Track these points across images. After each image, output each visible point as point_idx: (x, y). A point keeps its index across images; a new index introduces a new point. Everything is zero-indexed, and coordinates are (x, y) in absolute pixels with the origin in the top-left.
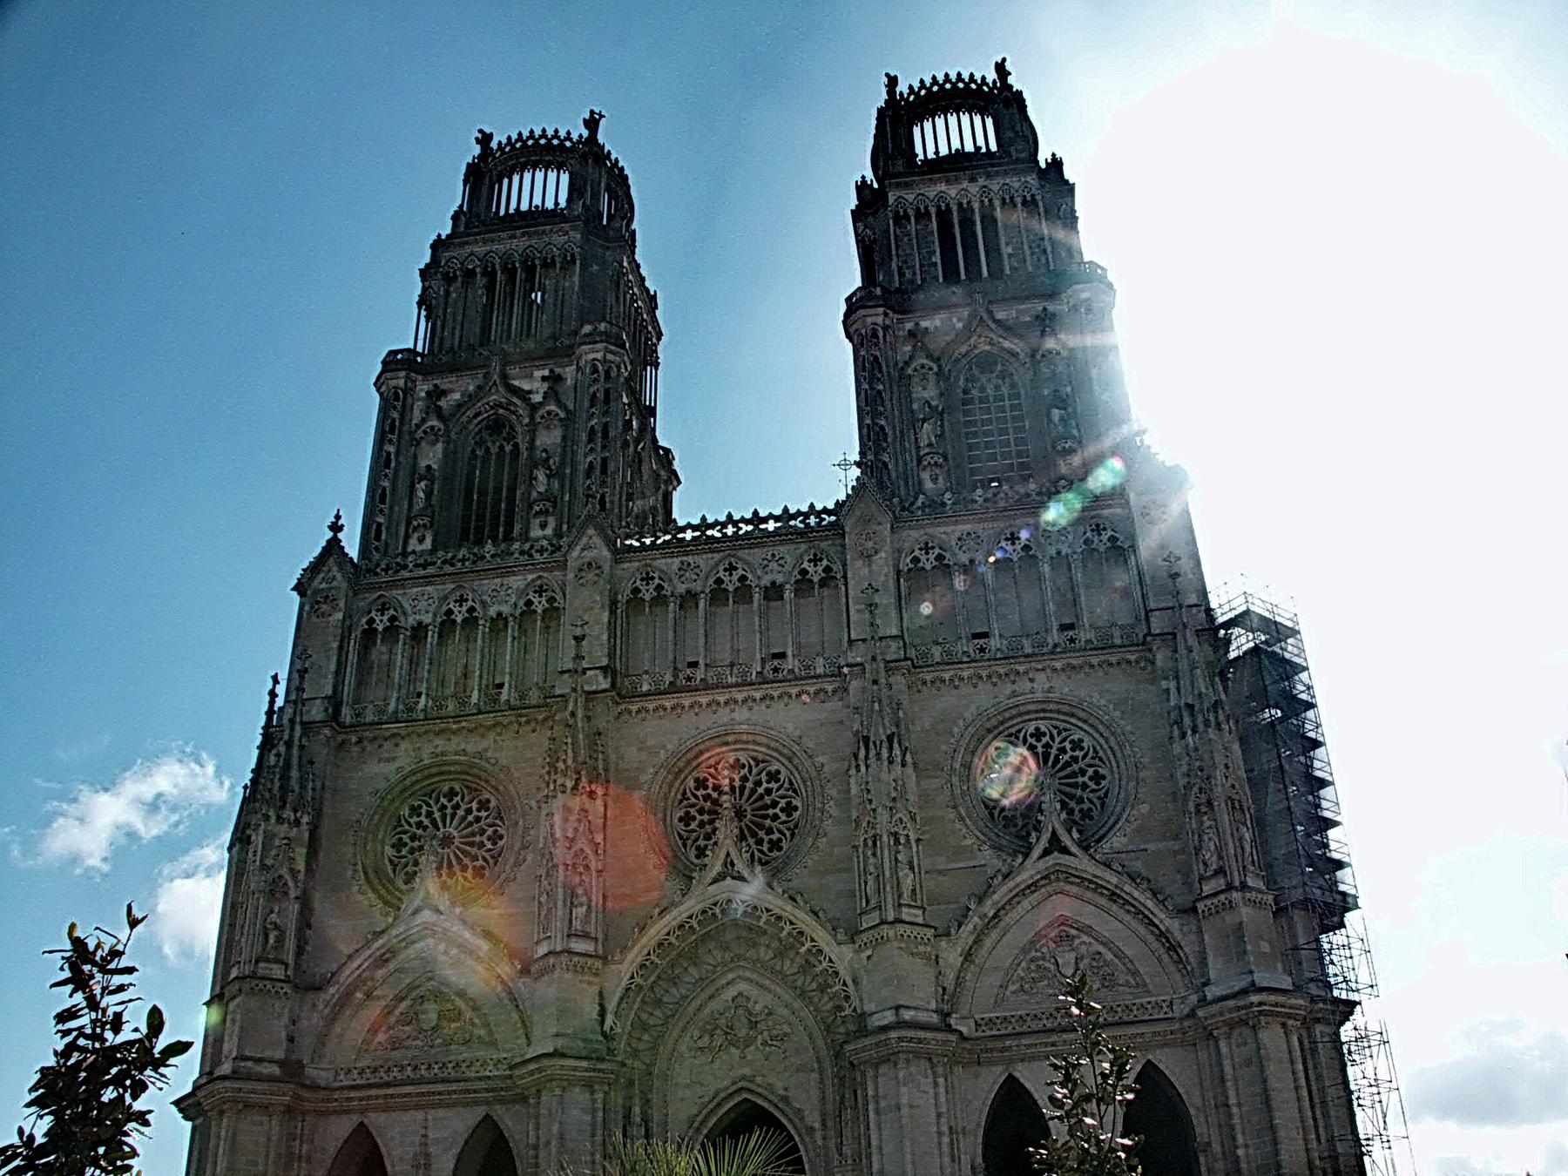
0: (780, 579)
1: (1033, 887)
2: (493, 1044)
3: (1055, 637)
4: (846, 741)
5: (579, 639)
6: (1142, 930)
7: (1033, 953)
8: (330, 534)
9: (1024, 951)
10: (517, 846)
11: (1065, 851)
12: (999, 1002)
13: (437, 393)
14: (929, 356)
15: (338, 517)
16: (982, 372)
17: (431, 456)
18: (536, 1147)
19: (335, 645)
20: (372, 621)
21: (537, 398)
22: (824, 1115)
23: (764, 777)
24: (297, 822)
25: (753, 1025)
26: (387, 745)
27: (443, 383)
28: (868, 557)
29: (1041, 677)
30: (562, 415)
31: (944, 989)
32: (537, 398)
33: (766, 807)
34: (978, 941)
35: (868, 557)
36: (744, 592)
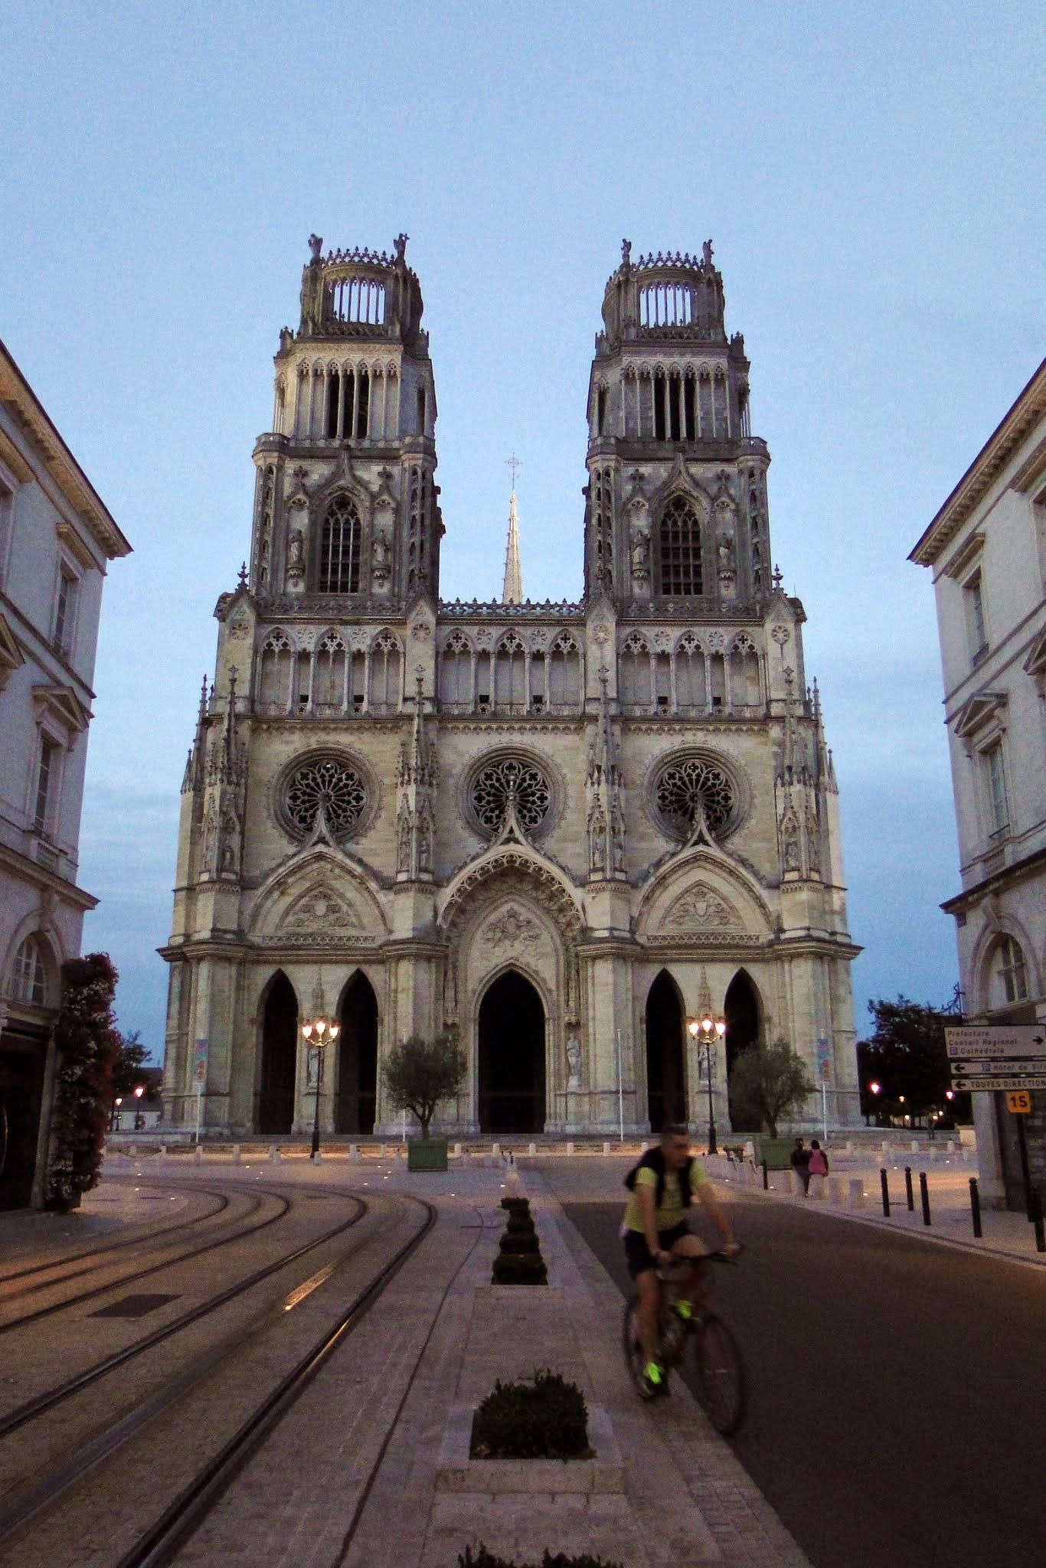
0: (543, 649)
1: (686, 863)
2: (363, 928)
3: (709, 709)
4: (582, 761)
5: (420, 680)
6: (746, 894)
7: (682, 901)
8: (240, 580)
9: (678, 899)
10: (376, 806)
11: (706, 843)
12: (662, 924)
13: (301, 474)
14: (644, 496)
15: (244, 567)
16: (676, 509)
17: (301, 521)
18: (396, 991)
19: (249, 661)
20: (270, 645)
21: (375, 488)
22: (558, 982)
23: (527, 777)
24: (238, 784)
25: (519, 927)
26: (286, 734)
27: (306, 464)
28: (601, 643)
29: (700, 735)
30: (393, 505)
31: (632, 918)
32: (375, 488)
33: (528, 795)
34: (653, 891)
35: (601, 643)
36: (519, 654)
